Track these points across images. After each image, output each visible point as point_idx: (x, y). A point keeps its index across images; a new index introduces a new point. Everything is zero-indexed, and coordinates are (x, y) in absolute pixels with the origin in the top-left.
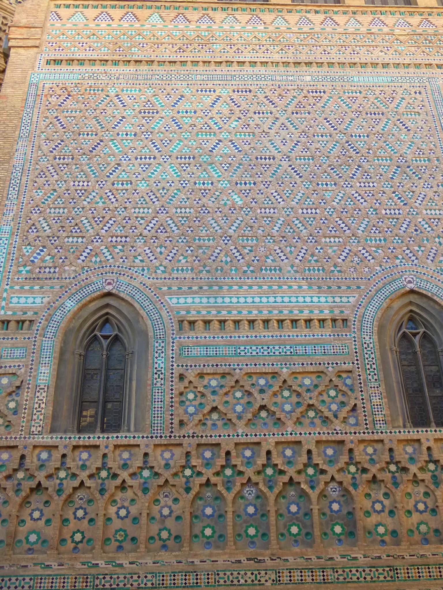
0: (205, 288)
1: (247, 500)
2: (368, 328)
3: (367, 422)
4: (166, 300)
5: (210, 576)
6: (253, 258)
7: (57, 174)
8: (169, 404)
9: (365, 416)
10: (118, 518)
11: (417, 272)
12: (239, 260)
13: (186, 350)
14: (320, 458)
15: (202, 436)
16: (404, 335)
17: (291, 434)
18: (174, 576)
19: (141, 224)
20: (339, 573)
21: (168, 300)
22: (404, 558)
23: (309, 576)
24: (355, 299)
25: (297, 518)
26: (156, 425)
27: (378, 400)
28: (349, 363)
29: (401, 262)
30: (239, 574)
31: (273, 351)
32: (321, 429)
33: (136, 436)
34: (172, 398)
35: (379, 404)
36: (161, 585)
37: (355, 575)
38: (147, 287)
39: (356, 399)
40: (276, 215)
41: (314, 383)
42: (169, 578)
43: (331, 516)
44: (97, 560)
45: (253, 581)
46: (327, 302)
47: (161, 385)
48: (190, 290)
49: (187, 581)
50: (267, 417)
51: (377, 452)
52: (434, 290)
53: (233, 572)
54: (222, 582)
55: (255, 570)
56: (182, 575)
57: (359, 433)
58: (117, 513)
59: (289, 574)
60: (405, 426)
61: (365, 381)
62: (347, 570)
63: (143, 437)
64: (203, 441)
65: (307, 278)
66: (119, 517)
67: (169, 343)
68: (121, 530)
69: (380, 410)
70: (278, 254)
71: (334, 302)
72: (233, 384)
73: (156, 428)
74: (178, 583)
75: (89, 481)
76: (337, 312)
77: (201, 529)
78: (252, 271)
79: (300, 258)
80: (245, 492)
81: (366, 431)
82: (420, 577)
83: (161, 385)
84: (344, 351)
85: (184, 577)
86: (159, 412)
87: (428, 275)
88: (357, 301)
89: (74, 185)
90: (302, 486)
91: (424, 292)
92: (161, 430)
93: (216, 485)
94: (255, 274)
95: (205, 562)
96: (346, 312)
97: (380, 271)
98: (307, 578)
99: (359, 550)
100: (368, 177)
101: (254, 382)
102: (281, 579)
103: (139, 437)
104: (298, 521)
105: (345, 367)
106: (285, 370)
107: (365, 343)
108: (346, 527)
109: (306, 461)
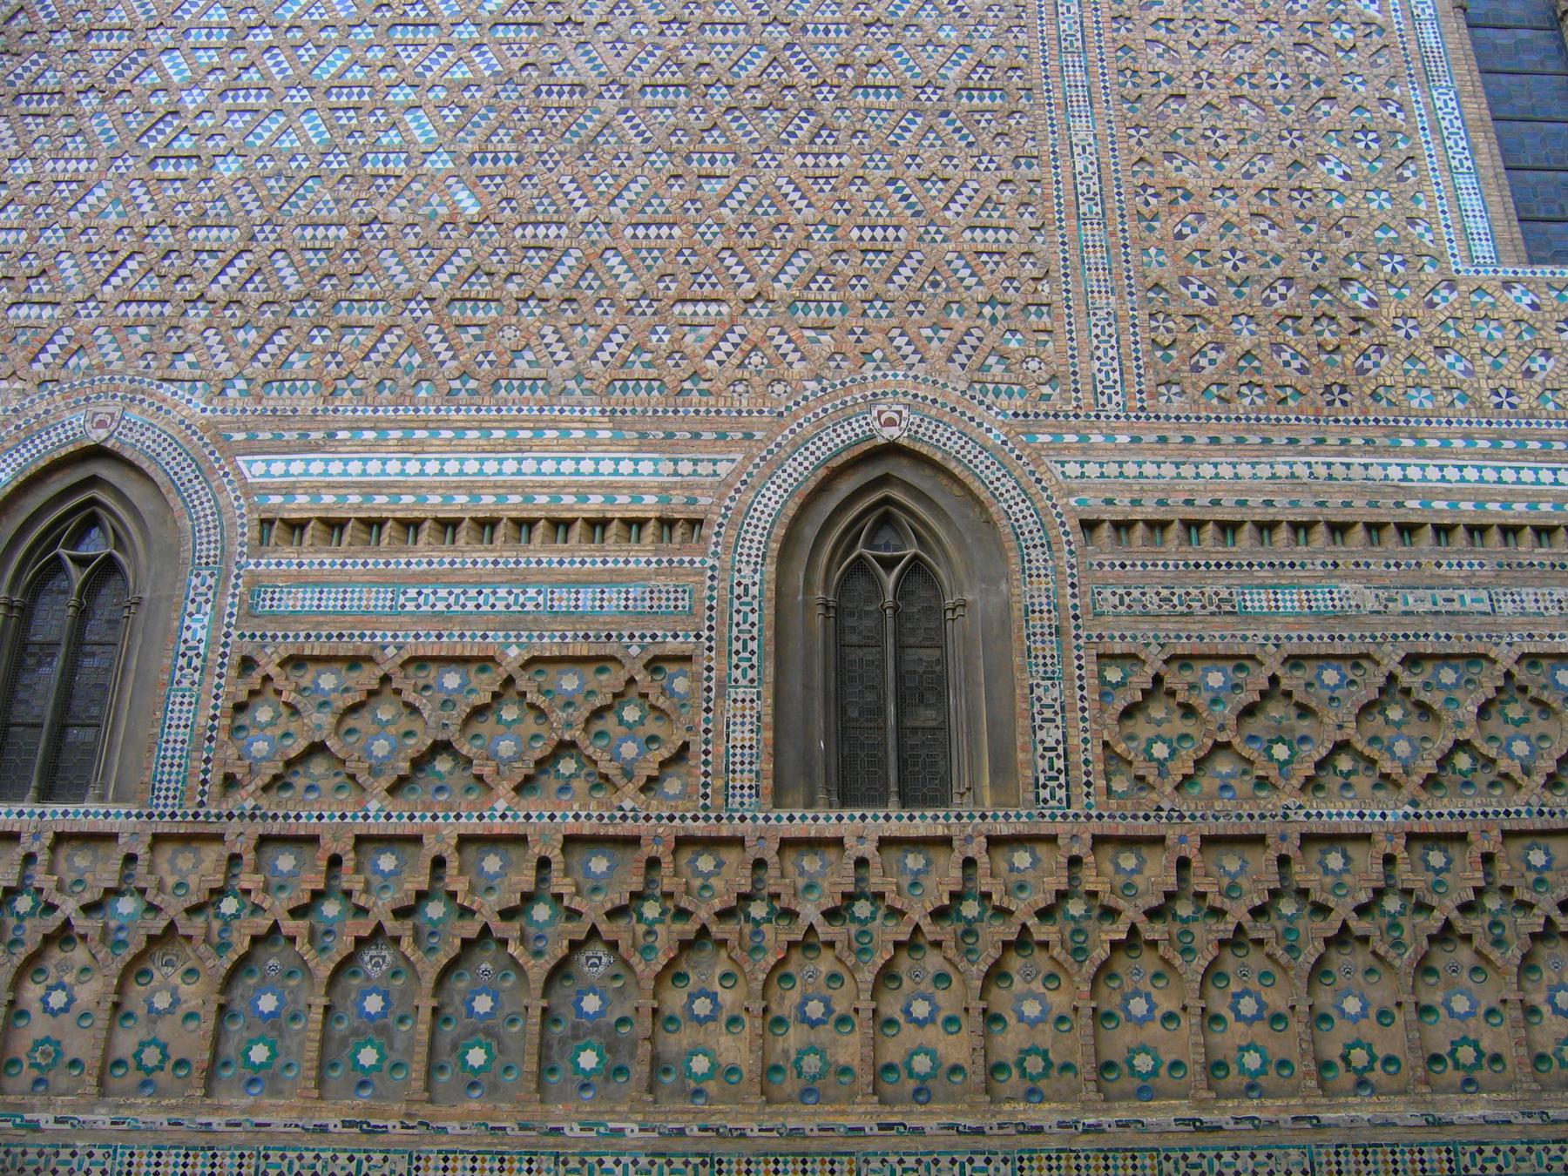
0: (341, 435)
1: (368, 978)
2: (755, 545)
3: (709, 791)
4: (238, 467)
5: (245, 1161)
6: (481, 357)
7: (17, 143)
8: (202, 734)
9: (706, 774)
11: (916, 396)
12: (442, 363)
13: (269, 595)
14: (568, 880)
15: (275, 817)
16: (860, 564)
18: (159, 1155)
19: (206, 269)
20: (570, 1166)
21: (243, 467)
22: (743, 1136)
24: (732, 466)
25: (489, 1032)
26: (164, 785)
27: (748, 735)
29: (878, 368)
30: (317, 1157)
31: (492, 600)
32: (584, 806)
33: (113, 811)
34: (214, 717)
35: (747, 744)
38: (194, 433)
39: (689, 729)
40: (560, 243)
41: (589, 687)
42: (145, 1159)
43: (575, 1027)
46: (656, 473)
48: (302, 441)
50: (451, 773)
51: (724, 869)
52: (953, 446)
56: (177, 1155)
57: (683, 818)
58: (44, 1000)
60: (810, 804)
61: (722, 686)
62: (592, 1160)
63: (128, 815)
64: (275, 828)
67: (227, 578)
68: (47, 1040)
70: (548, 346)
71: (676, 474)
72: (375, 685)
73: (163, 793)
76: (678, 498)
78: (473, 392)
79: (604, 356)
80: (367, 958)
83: (193, 683)
84: (680, 603)
85: (181, 1160)
86: (178, 753)
87: (944, 405)
88: (737, 473)
89: (54, 170)
90: (511, 949)
91: (924, 450)
92: (174, 797)
93: (292, 940)
94: (477, 399)
95: (238, 1125)
96: (704, 501)
97: (814, 393)
100: (830, 141)
101: (431, 682)
103: (118, 815)
105: (672, 646)
107: (739, 584)
108: (608, 1056)
109: (529, 887)
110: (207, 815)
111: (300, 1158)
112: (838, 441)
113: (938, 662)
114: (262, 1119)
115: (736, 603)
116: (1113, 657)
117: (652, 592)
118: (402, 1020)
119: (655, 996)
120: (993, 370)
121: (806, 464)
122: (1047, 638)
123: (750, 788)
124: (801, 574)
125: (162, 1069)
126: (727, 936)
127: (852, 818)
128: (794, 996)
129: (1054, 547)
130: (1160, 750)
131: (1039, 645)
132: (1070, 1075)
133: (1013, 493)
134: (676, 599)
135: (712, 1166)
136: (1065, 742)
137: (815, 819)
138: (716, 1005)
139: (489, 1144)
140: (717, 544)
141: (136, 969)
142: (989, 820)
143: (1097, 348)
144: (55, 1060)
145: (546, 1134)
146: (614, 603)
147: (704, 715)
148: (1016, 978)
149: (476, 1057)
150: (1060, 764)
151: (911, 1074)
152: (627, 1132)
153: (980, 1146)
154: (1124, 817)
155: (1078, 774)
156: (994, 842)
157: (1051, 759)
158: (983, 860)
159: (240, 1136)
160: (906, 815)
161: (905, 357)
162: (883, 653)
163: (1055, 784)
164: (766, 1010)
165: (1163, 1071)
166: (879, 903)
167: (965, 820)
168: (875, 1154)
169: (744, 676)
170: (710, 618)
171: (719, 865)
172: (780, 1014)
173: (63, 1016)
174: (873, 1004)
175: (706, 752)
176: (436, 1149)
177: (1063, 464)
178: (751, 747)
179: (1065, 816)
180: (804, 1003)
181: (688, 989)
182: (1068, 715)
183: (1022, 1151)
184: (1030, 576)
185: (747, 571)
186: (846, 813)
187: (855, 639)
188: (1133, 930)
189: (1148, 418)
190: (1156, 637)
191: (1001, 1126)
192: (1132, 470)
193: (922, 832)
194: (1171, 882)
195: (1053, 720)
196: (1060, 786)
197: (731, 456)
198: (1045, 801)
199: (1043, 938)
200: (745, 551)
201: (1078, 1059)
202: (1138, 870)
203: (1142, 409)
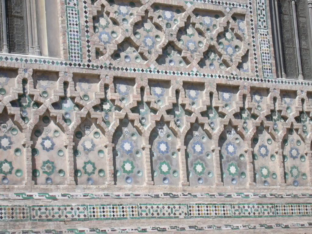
8: (83, 29)
10: (44, 149)
17: (196, 75)
22: (282, 197)
23: (213, 211)
27: (267, 49)
30: (158, 207)
36: (92, 217)
37: (247, 210)
44: (31, 192)
45: (169, 214)
47: (75, 5)
49: (115, 214)
53: (153, 206)
54: (144, 214)
55: (171, 204)
56: (110, 208)
59: (197, 209)
64: (119, 74)
66: (44, 148)
68: (48, 161)
74: (107, 215)
75: (13, 108)
77: (122, 164)
81: (257, 78)
82: (292, 213)
83: (75, 5)
85: (112, 210)
92: (78, 57)
95: (129, 195)
98: (212, 212)
102: (192, 212)
104: (201, 160)
106: (189, 5)
108: (239, 168)
110: (93, 66)
111: (152, 207)
114: (137, 193)
118: (173, 155)
125: (94, 173)
138: (267, 151)
139: (210, 201)
141: (78, 134)
144: (53, 170)
145: (226, 197)
149: (199, 168)
159: (130, 200)
173: (51, 151)
176: (195, 203)
180: (291, 151)
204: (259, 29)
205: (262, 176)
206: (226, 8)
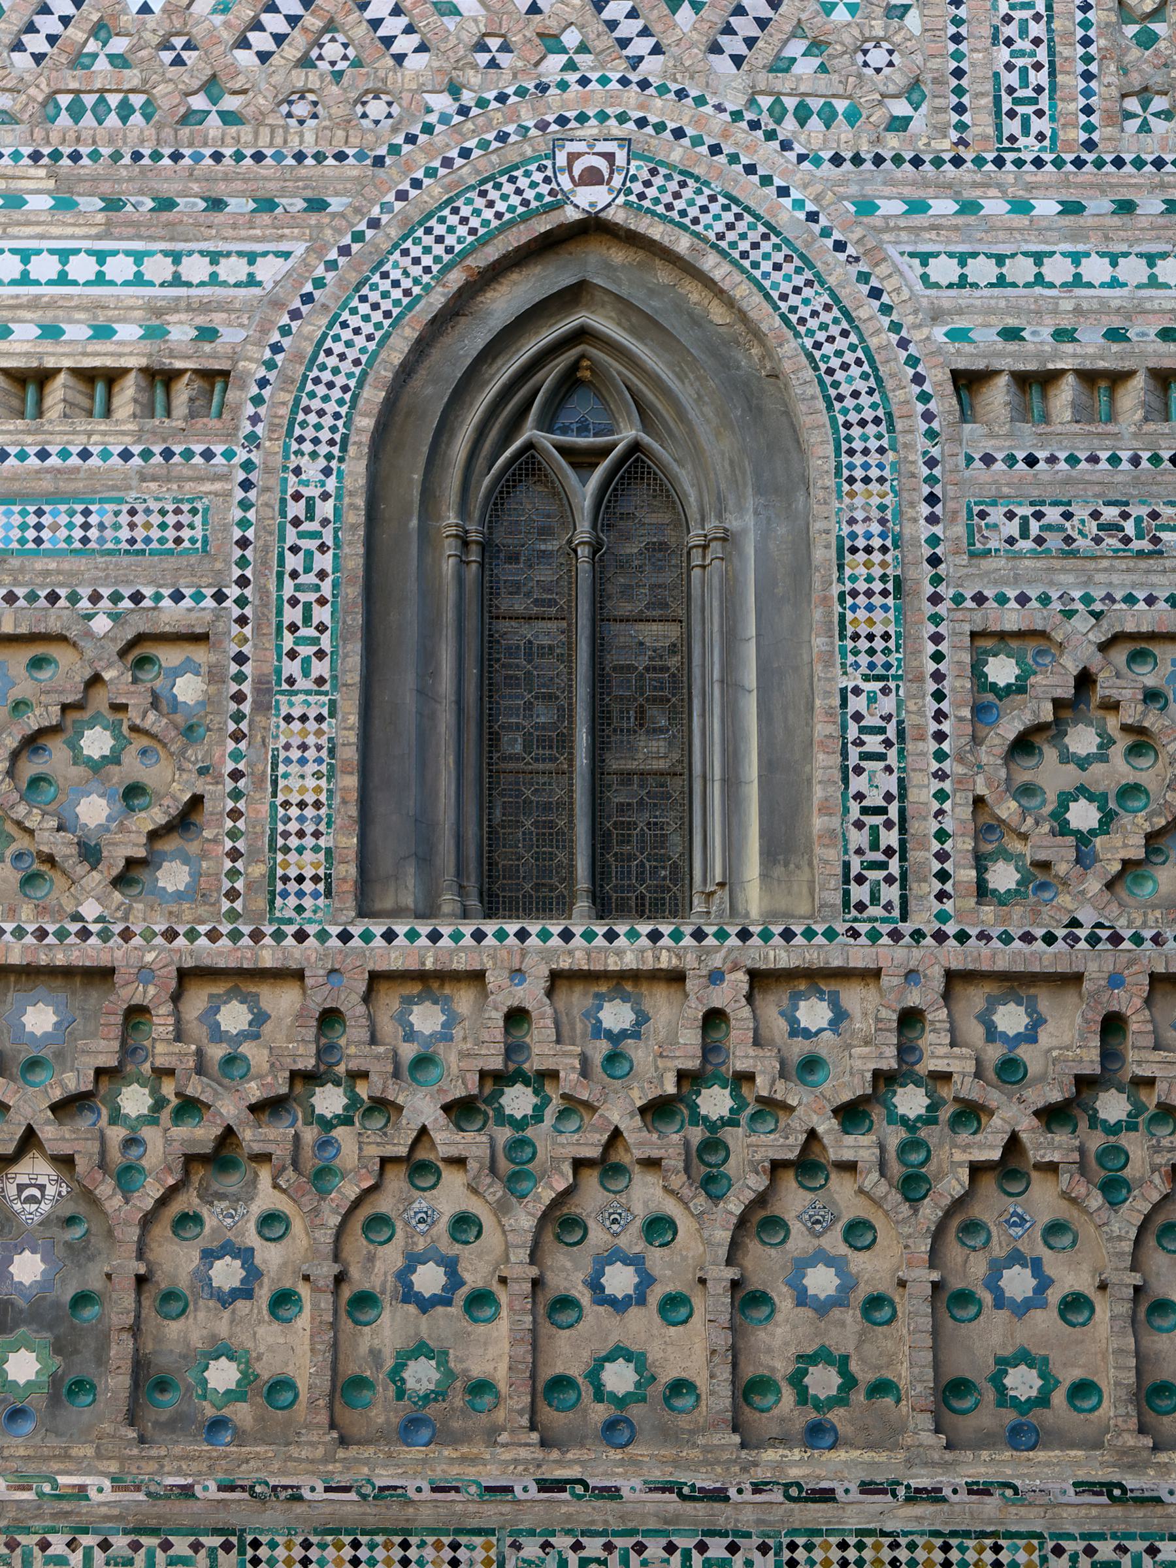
2: (328, 421)
3: (239, 885)
9: (234, 854)
11: (642, 123)
22: (297, 1498)
27: (311, 783)
28: (198, 597)
29: (571, 66)
35: (310, 798)
46: (139, 280)
51: (267, 1028)
57: (192, 935)
60: (429, 911)
61: (264, 689)
65: (56, 156)
69: (309, 828)
71: (177, 281)
76: (181, 332)
79: (36, 43)
81: (225, 928)
84: (186, 534)
97: (444, 119)
99: (99, 1456)
105: (171, 616)
107: (297, 496)
112: (488, 214)
113: (673, 649)
115: (291, 532)
116: (1002, 636)
117: (132, 512)
119: (140, 1255)
120: (797, 69)
121: (427, 260)
122: (877, 600)
123: (316, 879)
124: (417, 477)
126: (269, 1148)
127: (501, 935)
128: (391, 1257)
129: (899, 425)
130: (1083, 815)
131: (862, 614)
132: (889, 1401)
133: (826, 317)
134: (178, 526)
135: (242, 1552)
136: (903, 796)
137: (435, 936)
138: (253, 1273)
140: (255, 419)
142: (755, 941)
143: (1008, 19)
146: (63, 533)
147: (231, 745)
148: (796, 1227)
150: (890, 838)
151: (600, 1394)
152: (92, 1493)
153: (721, 1523)
154: (1006, 939)
155: (924, 857)
156: (759, 979)
157: (874, 829)
158: (741, 1014)
160: (601, 930)
161: (624, 43)
162: (570, 632)
163: (879, 875)
164: (340, 1279)
165: (1059, 1398)
166: (549, 1088)
167: (710, 941)
168: (532, 1533)
169: (306, 673)
170: (243, 562)
171: (260, 1018)
172: (366, 1286)
174: (534, 1272)
175: (235, 814)
177: (924, 258)
178: (317, 805)
179: (896, 935)
181: (201, 1243)
182: (910, 746)
183: (794, 1532)
184: (851, 480)
185: (312, 470)
186: (490, 927)
187: (519, 605)
188: (1013, 1144)
189: (1099, 164)
190: (1087, 599)
191: (757, 1489)
192: (1058, 270)
193: (630, 961)
194: (1089, 1060)
195: (881, 757)
196: (889, 880)
197: (284, 246)
198: (860, 907)
199: (847, 1155)
200: (309, 433)
201: (902, 1374)
202: (1030, 1036)
203: (1090, 145)
204: (282, 693)
205: (204, 1397)
206: (89, 617)
